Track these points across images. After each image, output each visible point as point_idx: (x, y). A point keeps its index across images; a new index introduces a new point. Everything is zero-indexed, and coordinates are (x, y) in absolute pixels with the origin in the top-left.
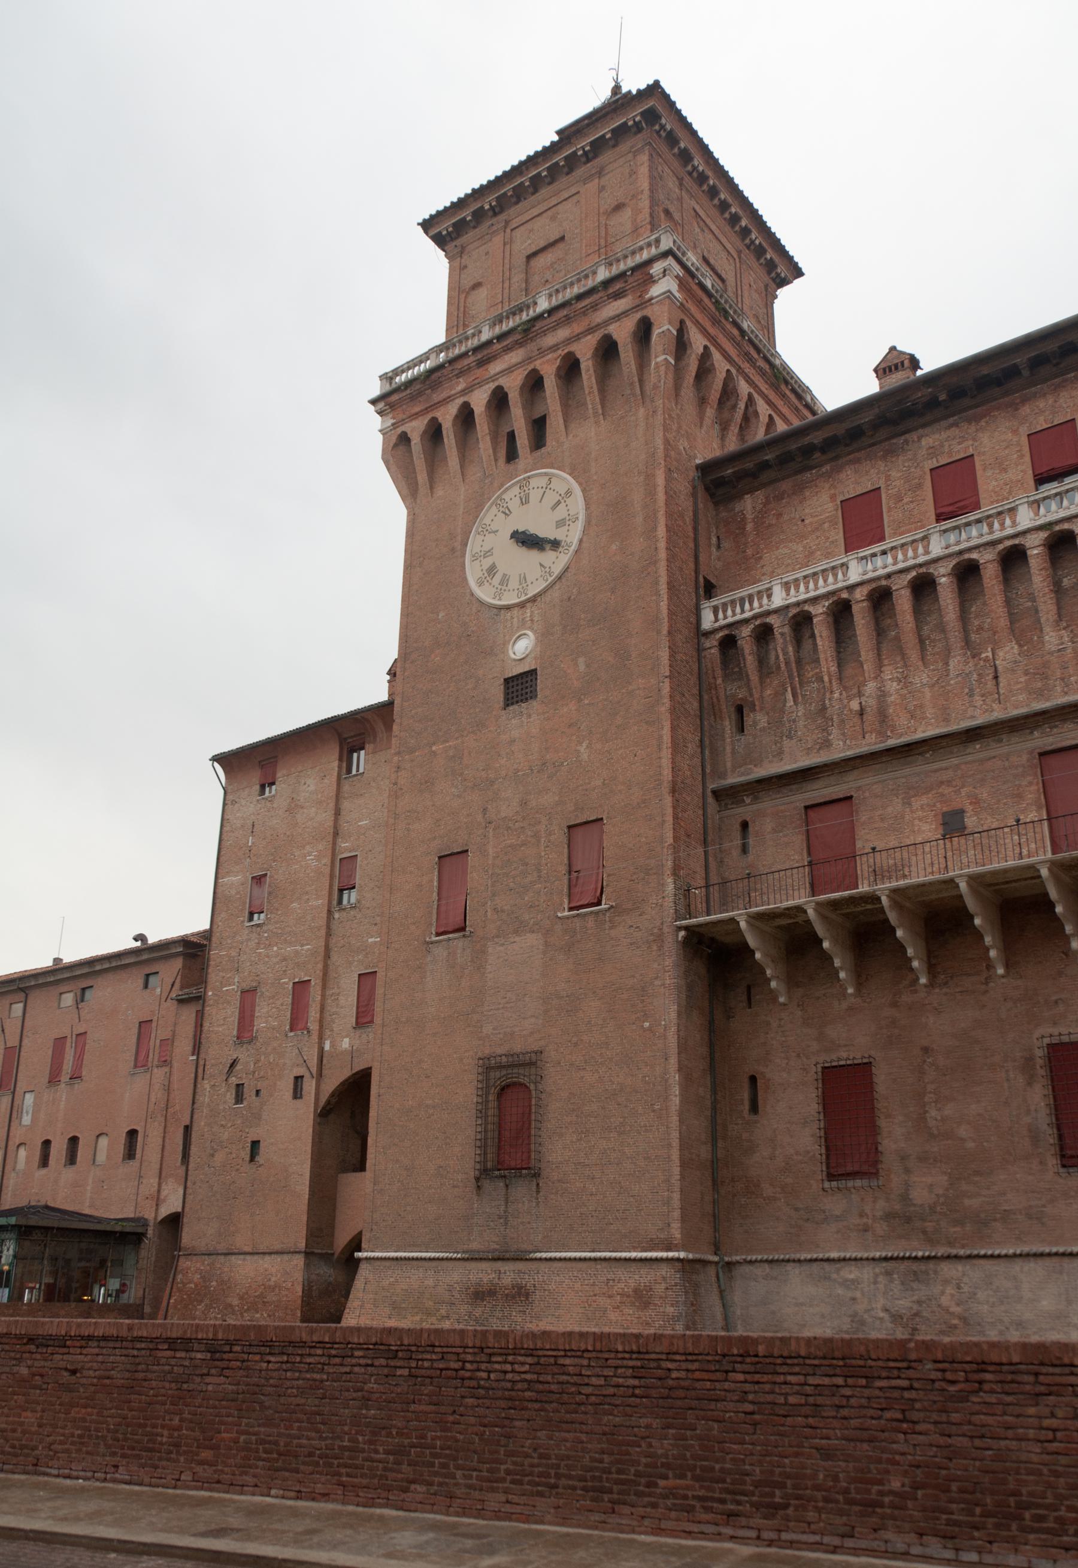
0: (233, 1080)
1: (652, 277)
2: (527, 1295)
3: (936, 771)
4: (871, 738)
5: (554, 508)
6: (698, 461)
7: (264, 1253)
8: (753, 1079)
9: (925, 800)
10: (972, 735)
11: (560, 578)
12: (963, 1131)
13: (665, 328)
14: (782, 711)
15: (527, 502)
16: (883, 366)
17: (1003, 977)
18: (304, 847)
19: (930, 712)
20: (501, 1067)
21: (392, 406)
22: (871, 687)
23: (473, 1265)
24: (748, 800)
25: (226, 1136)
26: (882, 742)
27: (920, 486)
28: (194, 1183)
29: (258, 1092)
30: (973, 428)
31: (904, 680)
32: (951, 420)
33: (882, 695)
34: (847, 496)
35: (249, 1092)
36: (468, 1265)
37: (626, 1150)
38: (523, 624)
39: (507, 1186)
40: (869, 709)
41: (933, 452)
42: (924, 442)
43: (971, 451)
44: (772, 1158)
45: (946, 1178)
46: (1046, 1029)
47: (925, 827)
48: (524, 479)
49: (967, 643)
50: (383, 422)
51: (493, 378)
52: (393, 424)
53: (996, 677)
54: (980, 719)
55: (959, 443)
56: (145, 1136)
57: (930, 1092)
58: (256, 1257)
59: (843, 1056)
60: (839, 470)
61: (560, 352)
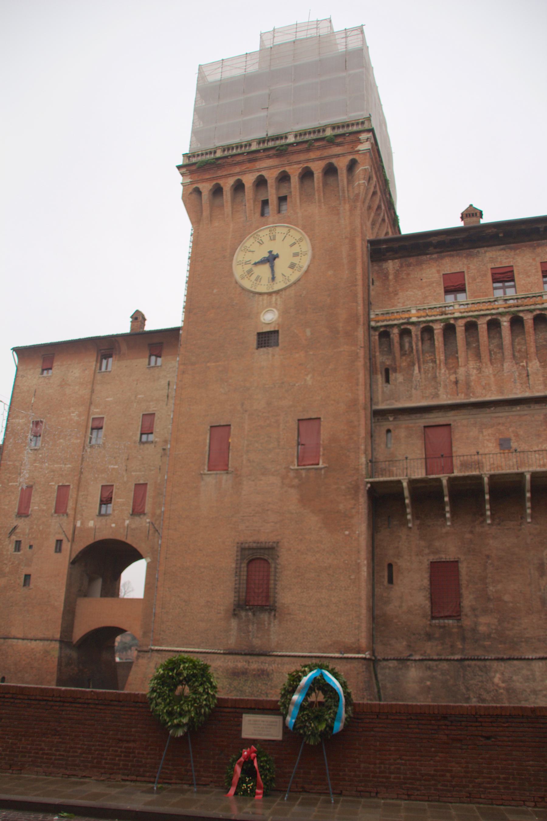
0: (14, 538)
1: (360, 140)
2: (268, 675)
3: (496, 417)
5: (291, 246)
6: (368, 238)
7: (31, 640)
8: (390, 566)
9: (490, 431)
11: (295, 283)
12: (507, 598)
13: (366, 167)
14: (412, 375)
15: (274, 239)
16: (465, 213)
17: (529, 523)
19: (493, 388)
20: (249, 549)
21: (192, 173)
22: (461, 371)
23: (230, 657)
24: (391, 419)
25: (7, 570)
26: (467, 399)
27: (485, 275)
29: (31, 547)
30: (512, 253)
31: (479, 369)
32: (502, 247)
33: (468, 375)
34: (446, 272)
35: (24, 546)
36: (226, 656)
37: (333, 599)
38: (270, 305)
40: (460, 381)
41: (492, 260)
42: (487, 254)
43: (511, 264)
44: (400, 607)
45: (496, 620)
47: (490, 445)
48: (273, 227)
50: (183, 179)
51: (259, 170)
52: (190, 182)
53: (528, 376)
54: (519, 396)
55: (506, 259)
57: (490, 578)
59: (444, 557)
60: (442, 258)
61: (301, 165)
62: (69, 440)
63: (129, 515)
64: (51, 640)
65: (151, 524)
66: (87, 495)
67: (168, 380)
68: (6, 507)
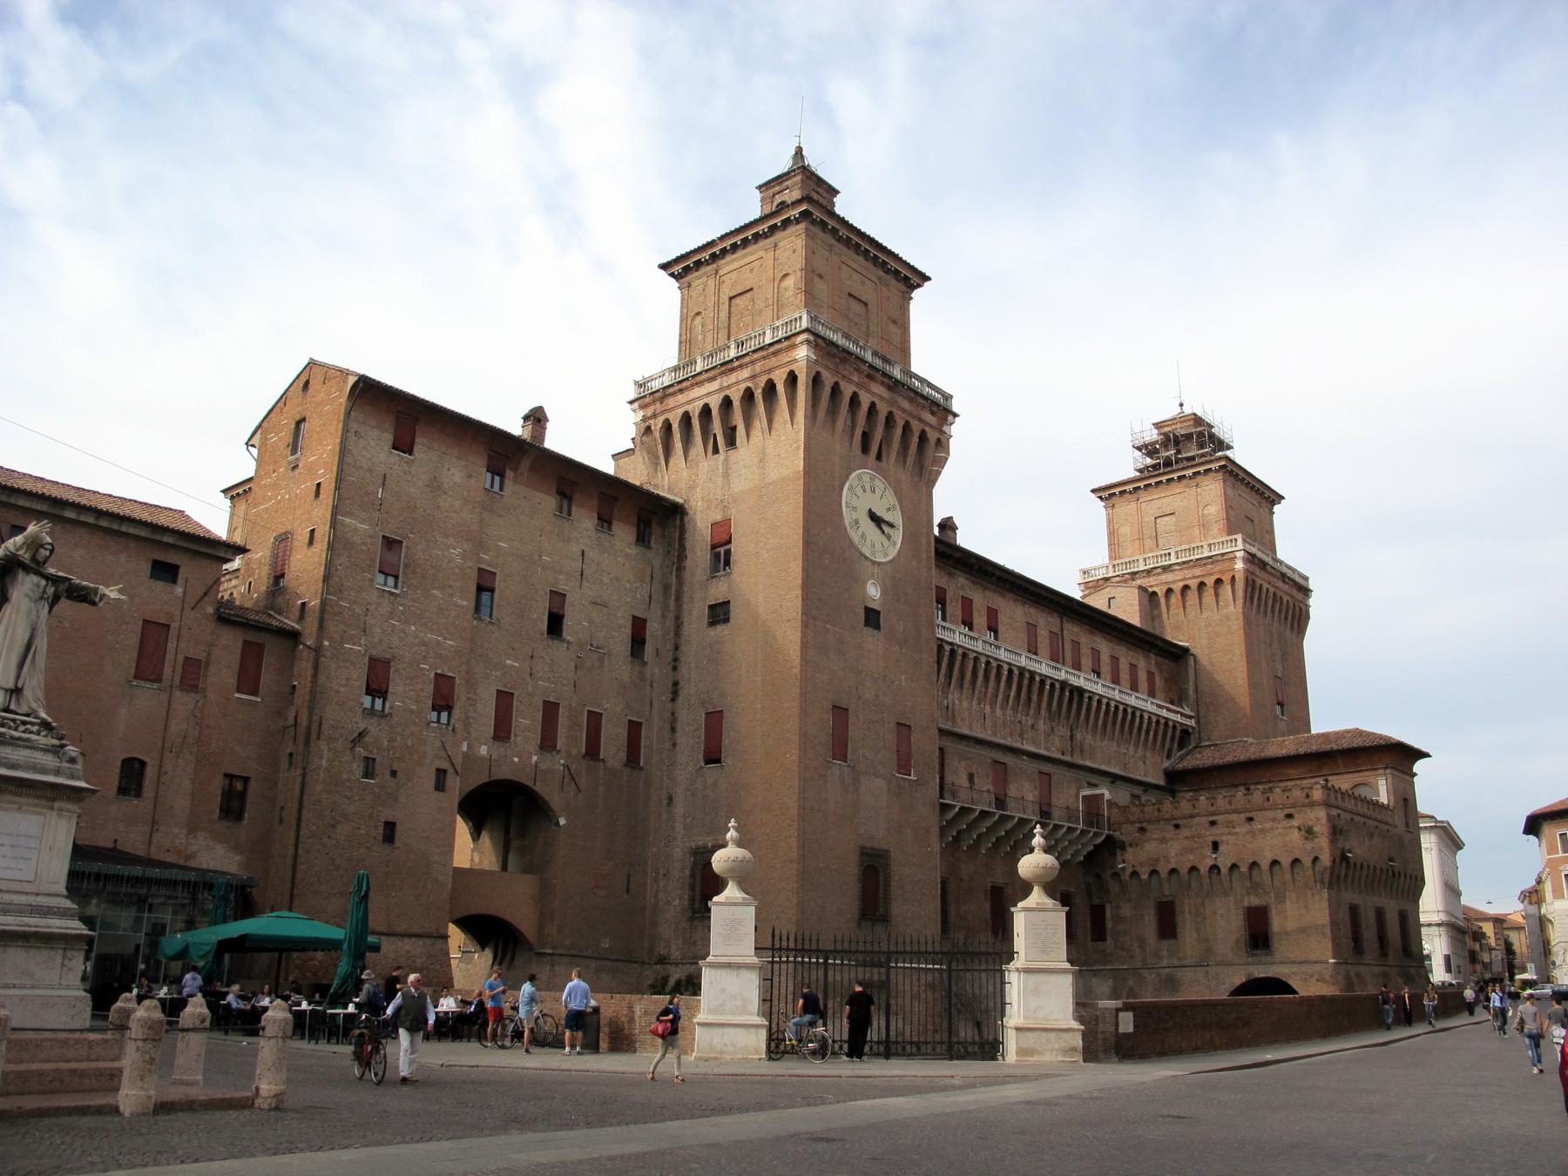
4: (950, 723)
10: (980, 742)
18: (448, 537)
22: (950, 696)
27: (957, 601)
28: (308, 852)
32: (968, 576)
33: (954, 704)
35: (382, 769)
38: (872, 577)
39: (873, 925)
46: (990, 880)
49: (978, 699)
51: (873, 394)
56: (160, 772)
58: (393, 939)
62: (451, 595)
63: (537, 748)
64: (435, 937)
65: (566, 769)
66: (475, 701)
67: (582, 547)
68: (342, 690)
